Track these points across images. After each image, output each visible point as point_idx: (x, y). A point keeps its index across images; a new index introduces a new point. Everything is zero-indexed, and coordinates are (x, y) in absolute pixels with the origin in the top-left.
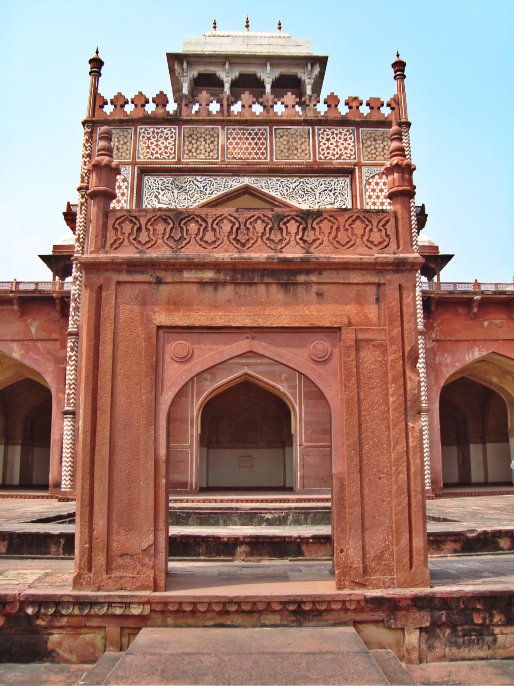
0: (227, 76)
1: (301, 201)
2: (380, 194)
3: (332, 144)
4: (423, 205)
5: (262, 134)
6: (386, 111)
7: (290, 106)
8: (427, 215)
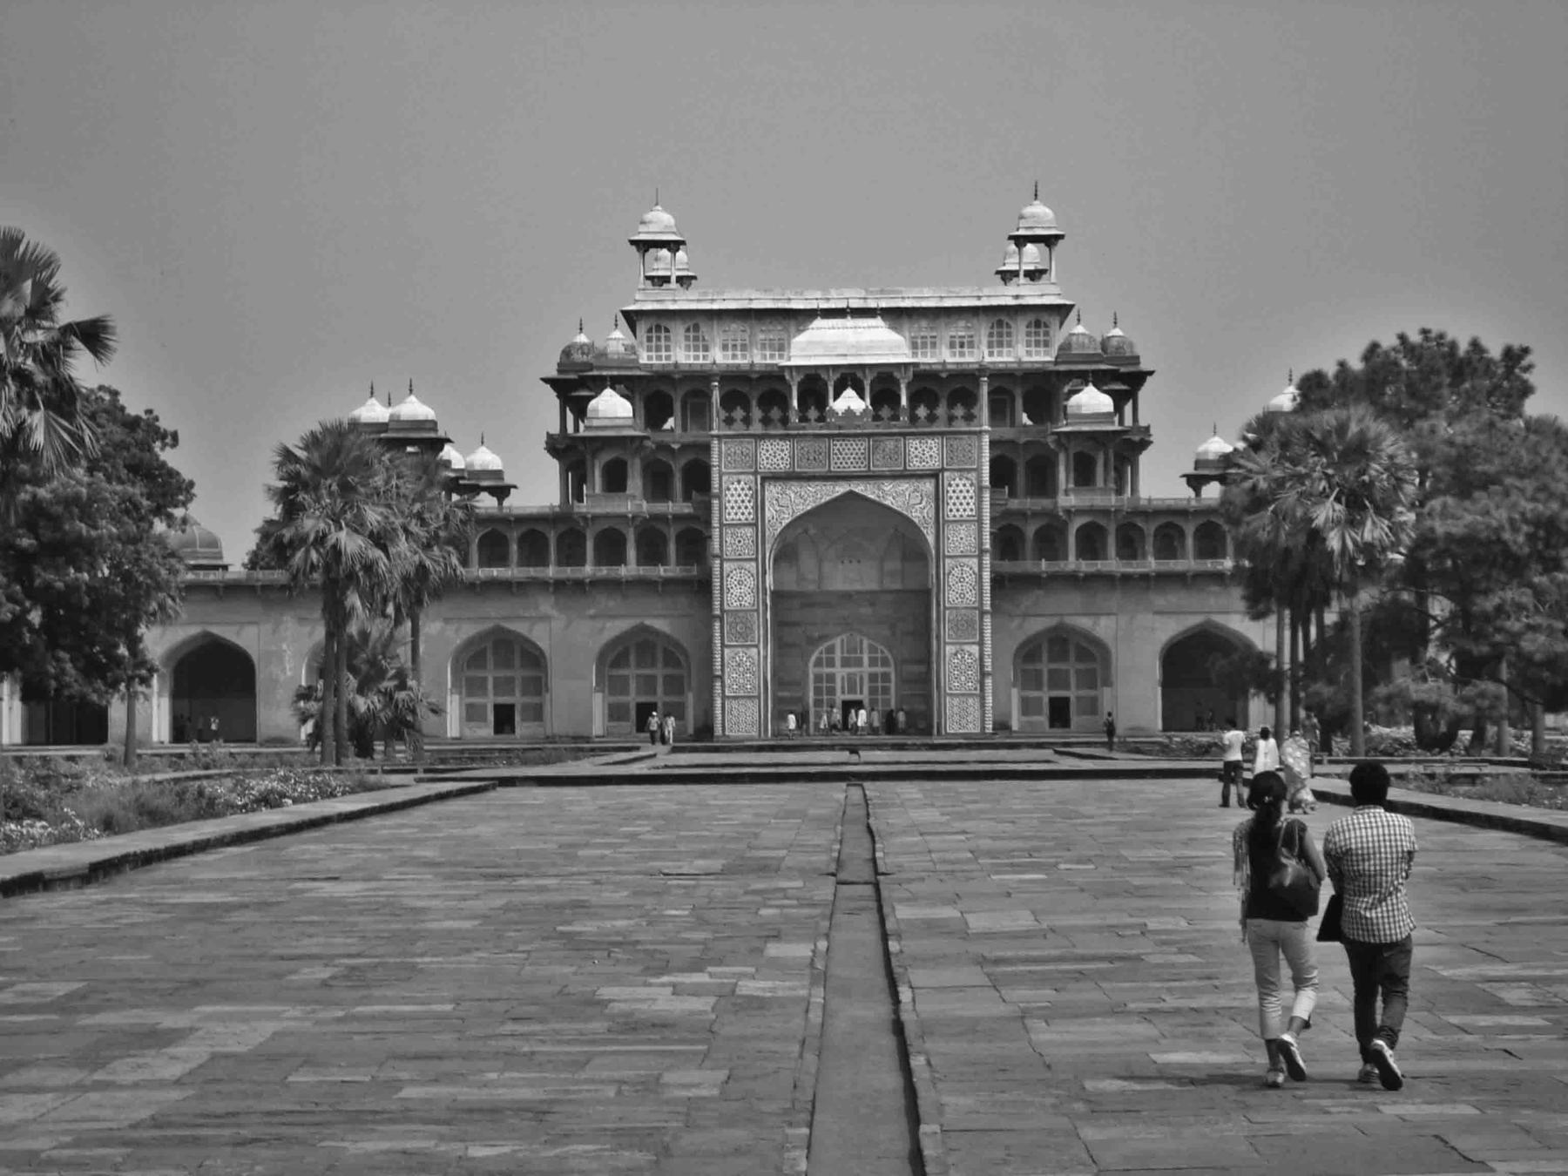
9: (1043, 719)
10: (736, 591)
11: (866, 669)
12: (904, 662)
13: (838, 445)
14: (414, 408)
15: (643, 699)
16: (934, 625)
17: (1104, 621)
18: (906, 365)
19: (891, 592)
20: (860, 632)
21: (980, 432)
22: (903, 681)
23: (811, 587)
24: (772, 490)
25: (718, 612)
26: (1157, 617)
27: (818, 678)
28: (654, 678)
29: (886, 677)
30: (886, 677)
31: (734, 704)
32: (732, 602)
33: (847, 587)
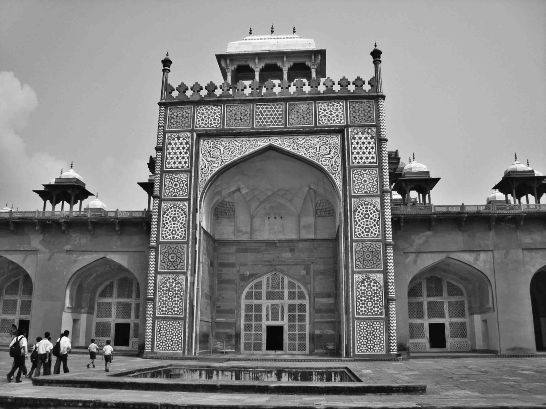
0: (257, 67)
1: (306, 153)
2: (362, 146)
3: (327, 113)
4: (397, 150)
5: (280, 108)
6: (367, 87)
7: (299, 87)
8: (400, 158)
9: (425, 341)
10: (170, 226)
11: (286, 301)
12: (317, 295)
13: (262, 108)
14: (71, 174)
15: (121, 321)
16: (343, 256)
17: (483, 256)
19: (306, 240)
20: (282, 272)
22: (316, 310)
23: (245, 237)
24: (206, 145)
25: (153, 244)
27: (249, 308)
28: (129, 305)
29: (302, 308)
30: (302, 308)
31: (163, 323)
32: (166, 235)
33: (272, 237)
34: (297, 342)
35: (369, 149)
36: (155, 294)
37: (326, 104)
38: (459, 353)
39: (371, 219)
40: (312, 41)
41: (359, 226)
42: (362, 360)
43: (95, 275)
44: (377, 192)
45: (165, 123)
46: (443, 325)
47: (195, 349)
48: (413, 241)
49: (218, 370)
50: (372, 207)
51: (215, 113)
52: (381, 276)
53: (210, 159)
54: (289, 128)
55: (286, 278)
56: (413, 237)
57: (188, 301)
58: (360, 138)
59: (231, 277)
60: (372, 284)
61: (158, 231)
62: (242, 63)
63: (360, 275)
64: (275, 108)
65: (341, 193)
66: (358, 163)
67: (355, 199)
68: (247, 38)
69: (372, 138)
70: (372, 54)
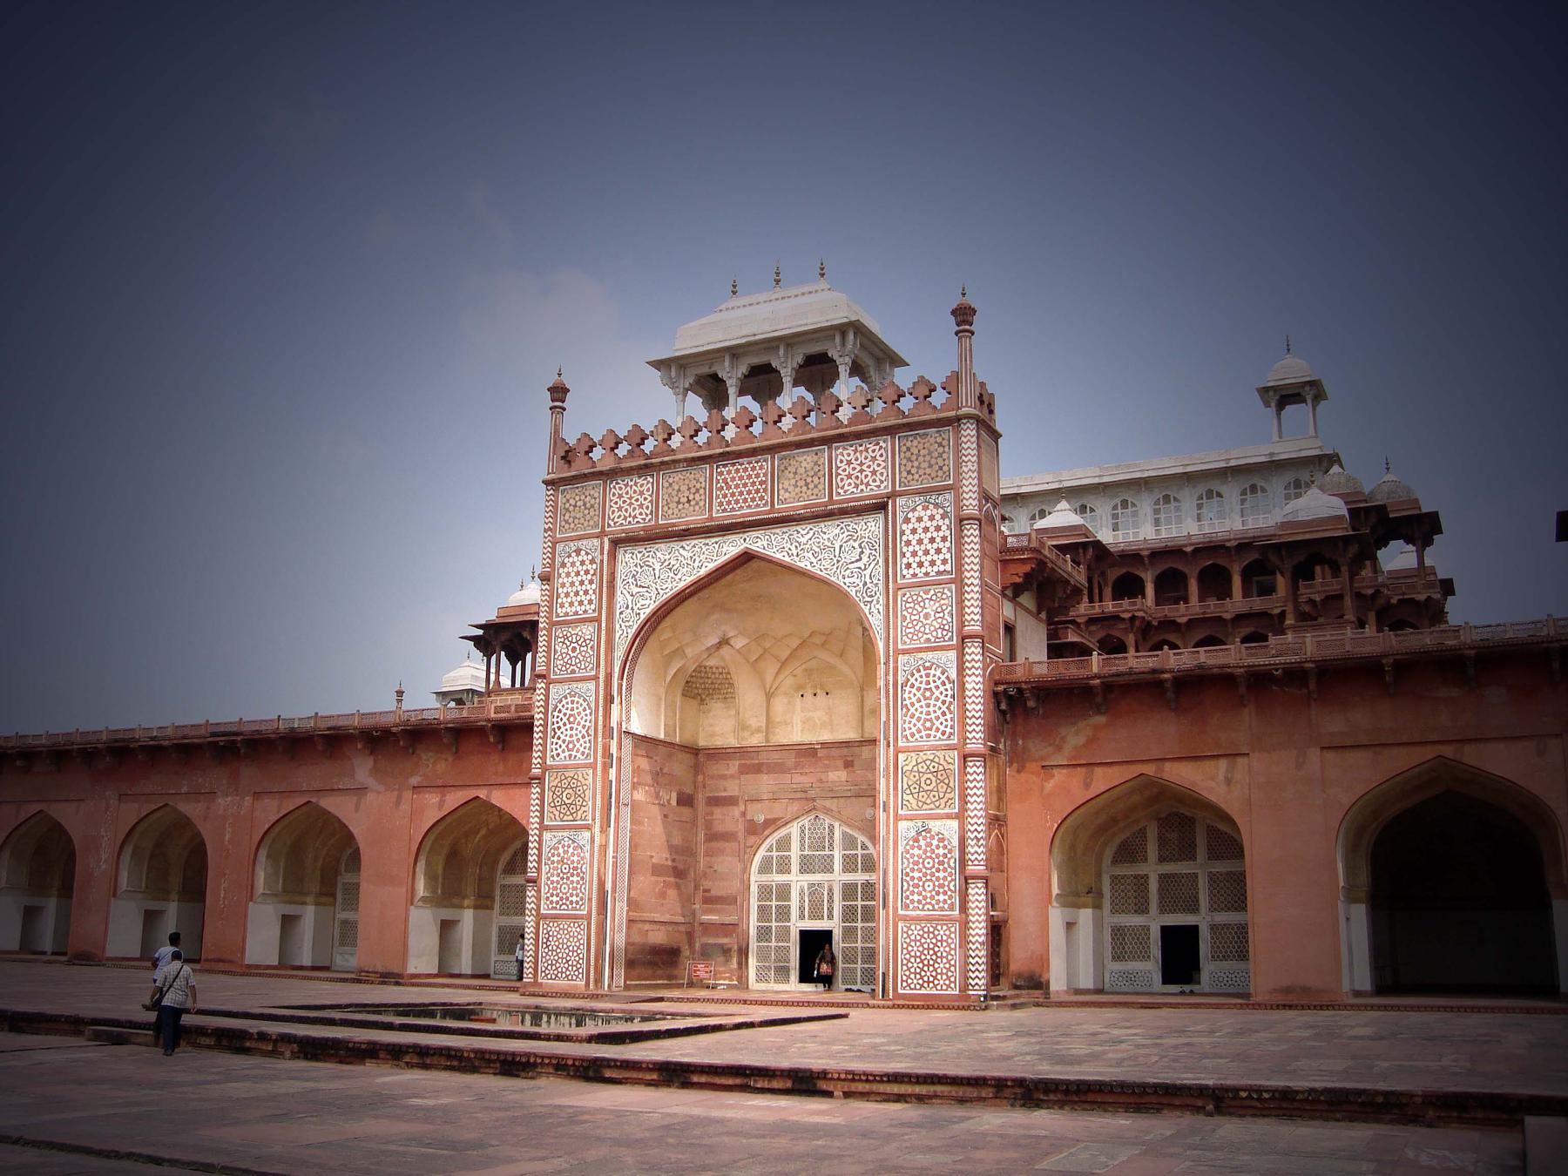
0: (732, 376)
9: (1150, 967)
10: (565, 733)
13: (728, 471)
18: (842, 329)
20: (827, 811)
21: (958, 419)
23: (755, 740)
24: (628, 559)
26: (1329, 755)
27: (765, 892)
31: (553, 927)
34: (859, 966)
35: (939, 544)
36: (539, 870)
37: (850, 450)
38: (1241, 997)
39: (937, 699)
40: (839, 297)
41: (912, 716)
42: (908, 1007)
43: (483, 832)
44: (951, 639)
45: (554, 524)
46: (1194, 930)
47: (614, 978)
48: (1063, 739)
49: (549, 1013)
50: (938, 673)
51: (642, 493)
52: (955, 824)
53: (636, 590)
54: (779, 511)
55: (836, 825)
56: (1063, 731)
57: (595, 883)
58: (920, 519)
59: (728, 826)
60: (935, 842)
61: (545, 745)
62: (705, 370)
63: (910, 824)
64: (753, 469)
65: (881, 645)
66: (915, 575)
67: (906, 657)
68: (723, 307)
69: (943, 517)
70: (954, 312)
